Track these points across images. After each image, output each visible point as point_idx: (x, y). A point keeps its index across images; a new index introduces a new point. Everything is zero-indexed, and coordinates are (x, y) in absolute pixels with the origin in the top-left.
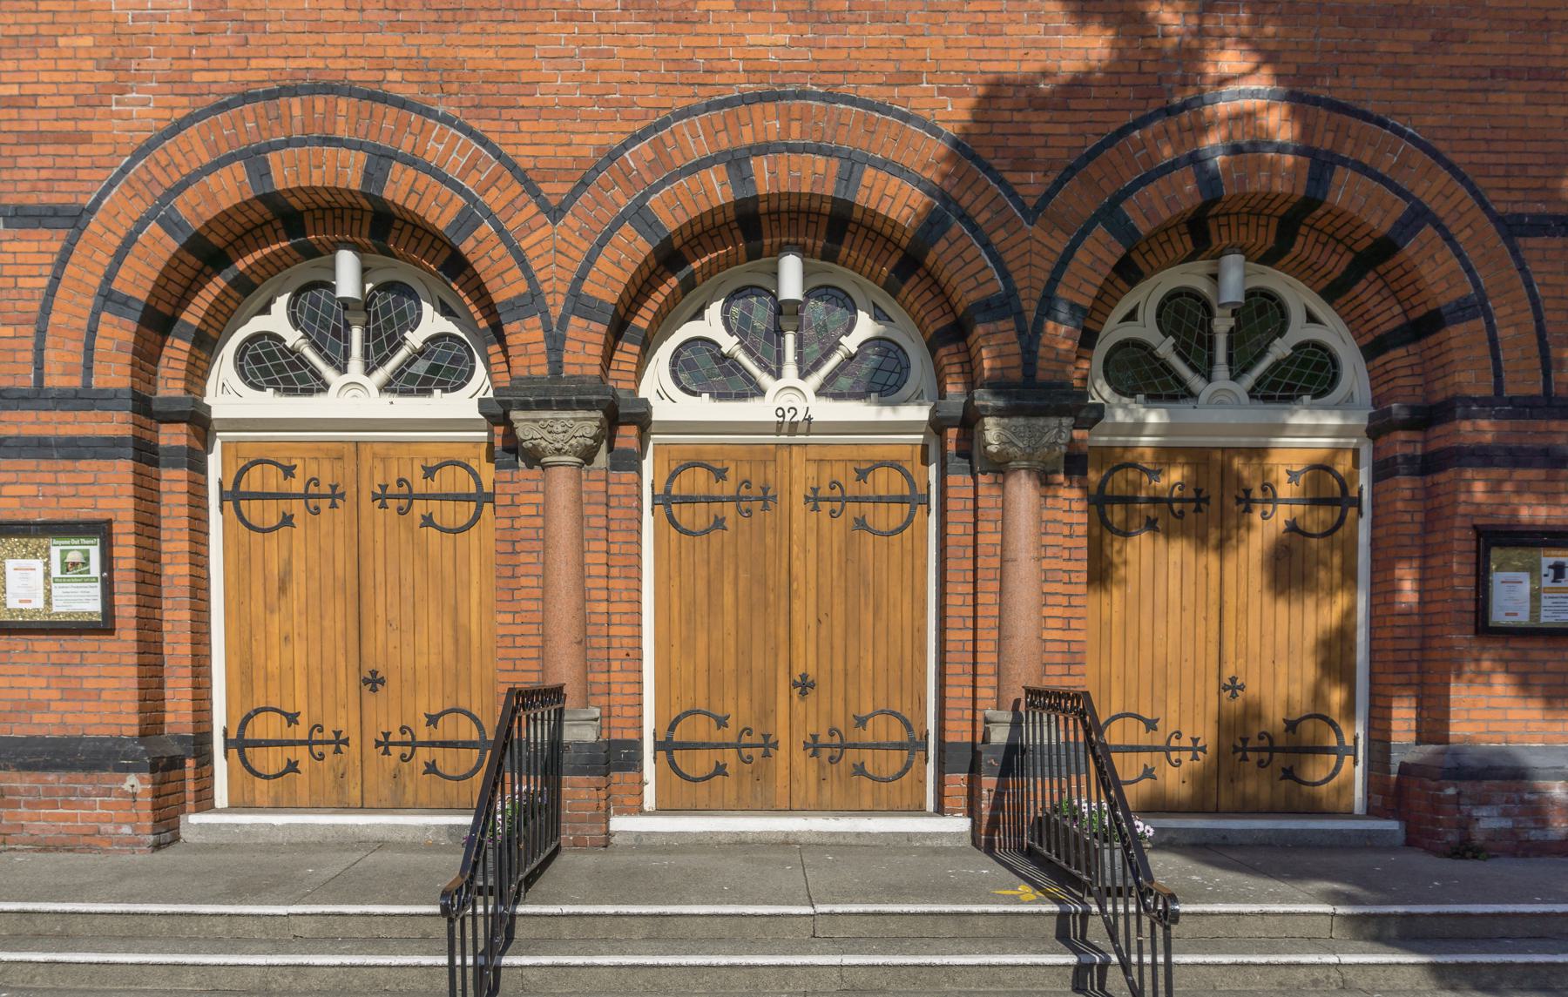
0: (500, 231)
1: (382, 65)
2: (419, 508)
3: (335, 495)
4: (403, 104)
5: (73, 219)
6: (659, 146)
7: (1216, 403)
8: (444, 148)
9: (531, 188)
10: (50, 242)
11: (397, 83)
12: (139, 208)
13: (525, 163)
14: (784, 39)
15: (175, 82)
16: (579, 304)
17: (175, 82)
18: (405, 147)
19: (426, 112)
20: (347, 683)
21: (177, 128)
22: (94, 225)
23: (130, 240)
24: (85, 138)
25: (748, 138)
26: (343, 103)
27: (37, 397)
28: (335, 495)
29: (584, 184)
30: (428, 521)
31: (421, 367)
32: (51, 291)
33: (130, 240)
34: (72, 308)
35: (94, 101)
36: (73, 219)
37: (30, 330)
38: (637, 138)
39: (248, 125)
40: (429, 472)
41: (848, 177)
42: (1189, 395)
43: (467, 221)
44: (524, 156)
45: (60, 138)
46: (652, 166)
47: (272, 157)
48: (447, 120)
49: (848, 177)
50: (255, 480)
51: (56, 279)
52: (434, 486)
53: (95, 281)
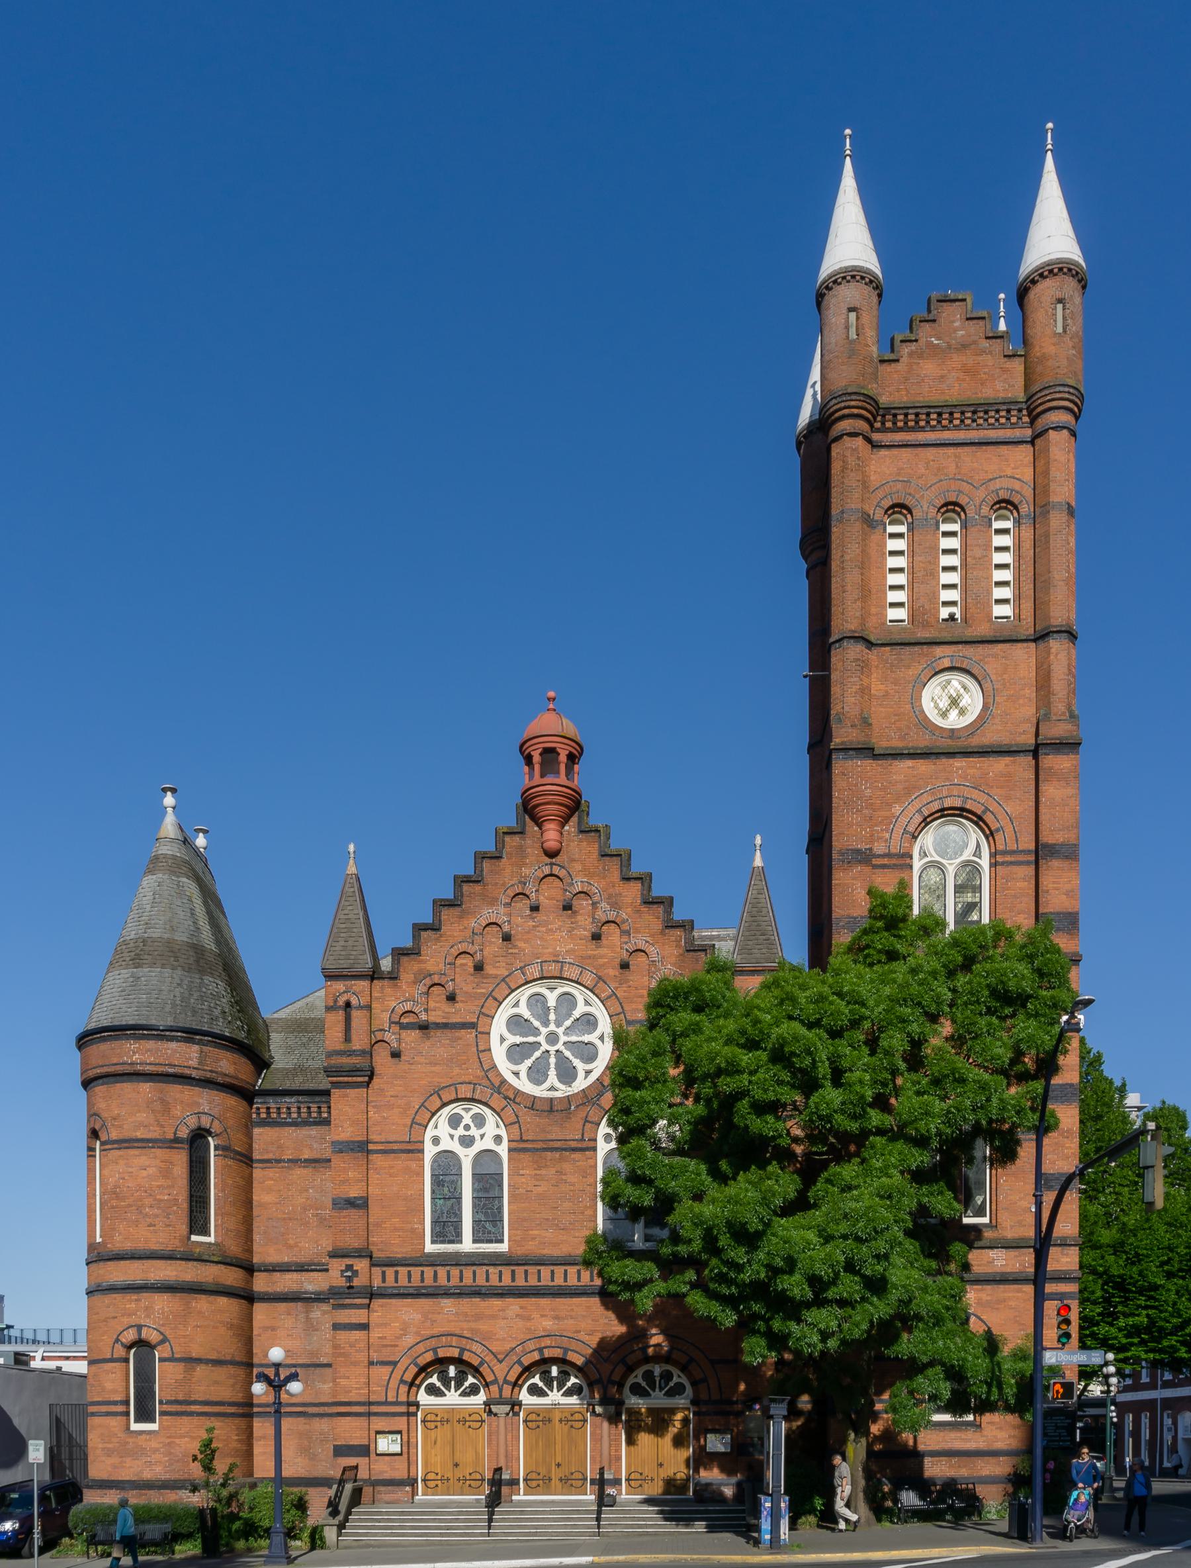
1: (462, 1329)
3: (448, 1421)
7: (655, 1398)
8: (476, 1347)
9: (495, 1356)
10: (390, 1369)
11: (466, 1334)
12: (409, 1362)
16: (506, 1381)
17: (418, 1333)
23: (407, 1368)
24: (397, 1346)
26: (454, 1338)
27: (386, 1403)
28: (448, 1421)
30: (470, 1427)
33: (407, 1368)
34: (394, 1383)
35: (399, 1338)
40: (470, 1415)
42: (649, 1395)
44: (494, 1349)
45: (392, 1346)
50: (429, 1418)
52: (471, 1418)
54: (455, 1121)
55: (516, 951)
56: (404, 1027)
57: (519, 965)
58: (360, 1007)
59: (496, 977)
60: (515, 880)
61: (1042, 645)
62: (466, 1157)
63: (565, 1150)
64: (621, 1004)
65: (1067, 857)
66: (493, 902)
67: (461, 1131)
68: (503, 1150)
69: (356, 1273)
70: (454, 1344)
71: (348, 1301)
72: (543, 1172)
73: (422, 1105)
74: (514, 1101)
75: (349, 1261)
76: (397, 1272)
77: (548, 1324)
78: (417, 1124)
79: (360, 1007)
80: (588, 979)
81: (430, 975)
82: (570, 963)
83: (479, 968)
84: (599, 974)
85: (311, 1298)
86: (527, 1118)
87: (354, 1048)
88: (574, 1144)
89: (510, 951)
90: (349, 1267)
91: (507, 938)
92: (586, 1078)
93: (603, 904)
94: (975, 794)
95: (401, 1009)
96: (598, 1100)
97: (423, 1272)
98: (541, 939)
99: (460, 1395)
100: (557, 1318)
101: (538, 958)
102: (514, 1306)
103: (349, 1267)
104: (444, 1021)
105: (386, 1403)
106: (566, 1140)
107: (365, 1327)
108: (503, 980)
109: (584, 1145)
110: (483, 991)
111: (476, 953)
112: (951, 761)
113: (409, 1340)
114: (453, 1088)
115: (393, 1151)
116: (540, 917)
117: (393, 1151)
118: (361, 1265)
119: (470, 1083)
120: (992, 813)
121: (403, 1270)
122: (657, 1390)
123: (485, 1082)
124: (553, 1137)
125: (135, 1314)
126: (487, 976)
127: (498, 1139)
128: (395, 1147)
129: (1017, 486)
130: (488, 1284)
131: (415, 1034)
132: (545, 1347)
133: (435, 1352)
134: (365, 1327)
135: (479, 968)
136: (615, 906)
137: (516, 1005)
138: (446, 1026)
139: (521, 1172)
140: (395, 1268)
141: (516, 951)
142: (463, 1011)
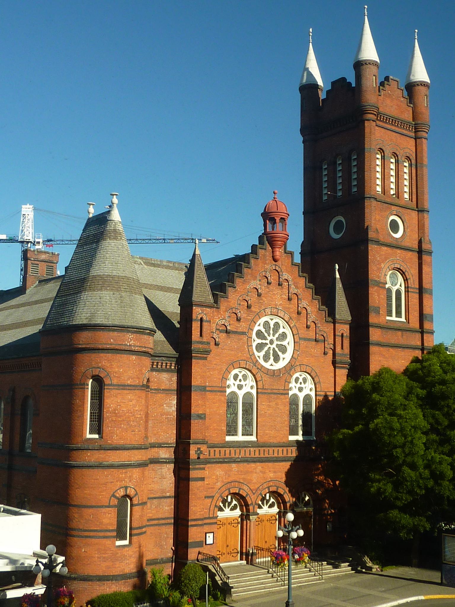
0: (249, 496)
1: (240, 479)
2: (221, 523)
4: (242, 483)
5: (213, 497)
6: (262, 486)
8: (245, 488)
10: (210, 500)
12: (219, 496)
13: (252, 489)
14: (273, 475)
15: (223, 481)
17: (223, 481)
18: (242, 488)
19: (244, 484)
20: (225, 546)
21: (222, 486)
22: (215, 497)
23: (218, 499)
24: (214, 488)
25: (270, 485)
26: (237, 483)
29: (256, 491)
31: (232, 508)
32: (210, 506)
33: (218, 499)
36: (213, 497)
37: (208, 510)
38: (261, 486)
39: (228, 486)
41: (277, 489)
43: (247, 495)
44: (252, 488)
45: (212, 488)
46: (262, 489)
47: (231, 489)
48: (245, 484)
49: (277, 489)
51: (211, 504)
53: (215, 504)
54: (236, 377)
55: (262, 301)
56: (221, 331)
57: (263, 307)
58: (207, 321)
59: (255, 312)
60: (263, 270)
61: (420, 213)
62: (241, 394)
63: (279, 394)
64: (297, 330)
65: (430, 294)
66: (255, 279)
67: (237, 382)
68: (254, 391)
69: (201, 452)
70: (237, 486)
71: (197, 466)
72: (270, 404)
73: (226, 369)
74: (261, 370)
75: (199, 446)
76: (215, 451)
77: (272, 475)
78: (224, 378)
79: (207, 321)
80: (287, 317)
81: (232, 308)
82: (281, 310)
83: (249, 307)
84: (291, 316)
85: (164, 462)
86: (266, 378)
87: (204, 341)
88: (281, 392)
89: (260, 301)
90: (199, 449)
91: (259, 295)
92: (283, 360)
93: (293, 286)
94: (403, 264)
95: (220, 323)
96: (290, 372)
97: (225, 451)
98: (271, 297)
99: (230, 510)
100: (275, 472)
101: (270, 306)
102: (259, 466)
103: (199, 449)
104: (235, 330)
105: (209, 518)
106: (279, 389)
107: (203, 479)
108: (257, 314)
109: (285, 392)
110: (250, 318)
111: (249, 300)
112: (397, 250)
113: (219, 484)
114: (238, 362)
115: (215, 391)
116: (271, 287)
117: (215, 391)
118: (204, 448)
119: (245, 360)
120: (407, 272)
121: (217, 450)
122: (301, 503)
123: (250, 360)
124: (275, 388)
125: (124, 481)
126: (252, 312)
127: (252, 387)
128: (216, 389)
129: (411, 153)
130: (250, 456)
131: (224, 335)
132: (271, 486)
133: (229, 491)
134: (203, 479)
135: (249, 307)
136: (297, 287)
137: (259, 325)
138: (236, 333)
139: (263, 403)
140: (214, 449)
141: (262, 301)
142: (242, 326)
